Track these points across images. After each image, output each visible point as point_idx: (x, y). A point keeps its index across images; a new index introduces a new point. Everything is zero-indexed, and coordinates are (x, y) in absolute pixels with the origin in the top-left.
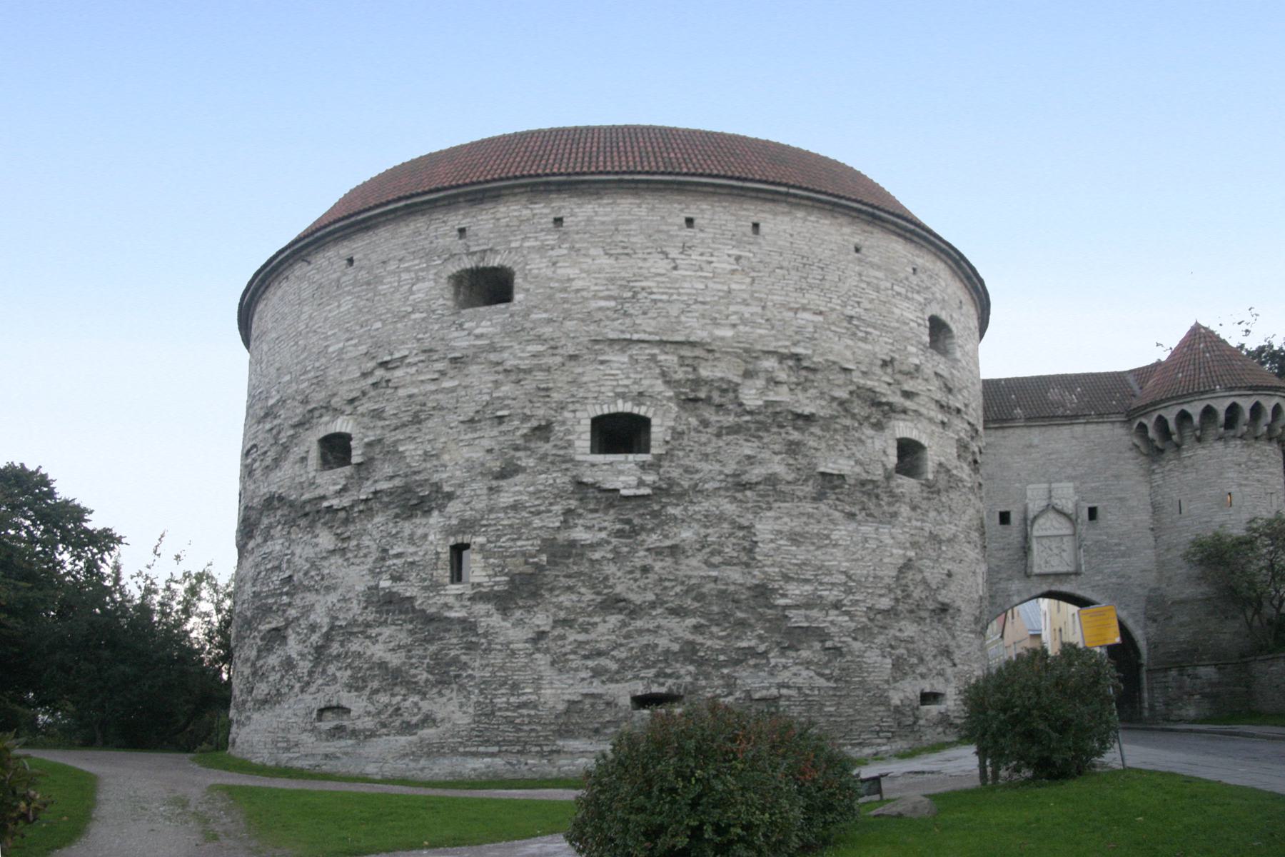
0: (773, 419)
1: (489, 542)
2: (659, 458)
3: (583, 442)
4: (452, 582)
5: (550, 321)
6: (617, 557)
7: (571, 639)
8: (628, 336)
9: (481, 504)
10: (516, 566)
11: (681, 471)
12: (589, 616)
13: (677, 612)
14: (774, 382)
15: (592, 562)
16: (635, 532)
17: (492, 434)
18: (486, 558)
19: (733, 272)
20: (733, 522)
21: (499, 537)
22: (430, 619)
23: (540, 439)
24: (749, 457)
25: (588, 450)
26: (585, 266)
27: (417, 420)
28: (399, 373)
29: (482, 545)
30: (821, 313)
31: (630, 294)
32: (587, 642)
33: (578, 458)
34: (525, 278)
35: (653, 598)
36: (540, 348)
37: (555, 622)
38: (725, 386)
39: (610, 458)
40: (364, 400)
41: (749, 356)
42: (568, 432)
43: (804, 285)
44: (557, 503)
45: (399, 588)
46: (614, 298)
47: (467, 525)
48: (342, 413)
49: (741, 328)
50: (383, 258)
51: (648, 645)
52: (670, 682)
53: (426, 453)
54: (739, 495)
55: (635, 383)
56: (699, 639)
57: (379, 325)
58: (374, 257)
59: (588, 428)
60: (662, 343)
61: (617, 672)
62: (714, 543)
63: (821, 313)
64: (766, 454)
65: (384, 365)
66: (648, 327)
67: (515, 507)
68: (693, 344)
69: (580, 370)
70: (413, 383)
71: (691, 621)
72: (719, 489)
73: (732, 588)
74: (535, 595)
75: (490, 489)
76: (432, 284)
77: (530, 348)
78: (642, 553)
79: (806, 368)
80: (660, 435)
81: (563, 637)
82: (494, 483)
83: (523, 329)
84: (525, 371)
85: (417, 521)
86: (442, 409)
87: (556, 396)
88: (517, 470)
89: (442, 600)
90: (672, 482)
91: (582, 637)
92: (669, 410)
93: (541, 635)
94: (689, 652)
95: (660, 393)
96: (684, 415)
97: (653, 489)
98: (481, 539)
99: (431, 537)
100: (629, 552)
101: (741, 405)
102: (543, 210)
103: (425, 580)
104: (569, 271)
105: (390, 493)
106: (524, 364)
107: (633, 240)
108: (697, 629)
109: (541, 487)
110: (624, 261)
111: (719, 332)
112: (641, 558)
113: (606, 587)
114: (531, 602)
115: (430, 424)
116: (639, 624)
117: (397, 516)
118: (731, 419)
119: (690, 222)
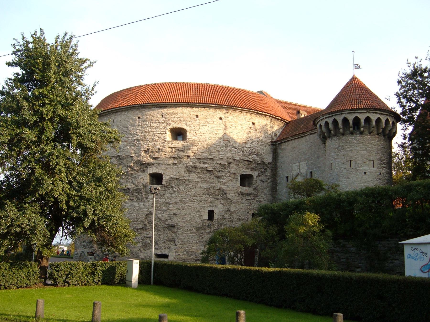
30: (126, 141)
63: (126, 141)
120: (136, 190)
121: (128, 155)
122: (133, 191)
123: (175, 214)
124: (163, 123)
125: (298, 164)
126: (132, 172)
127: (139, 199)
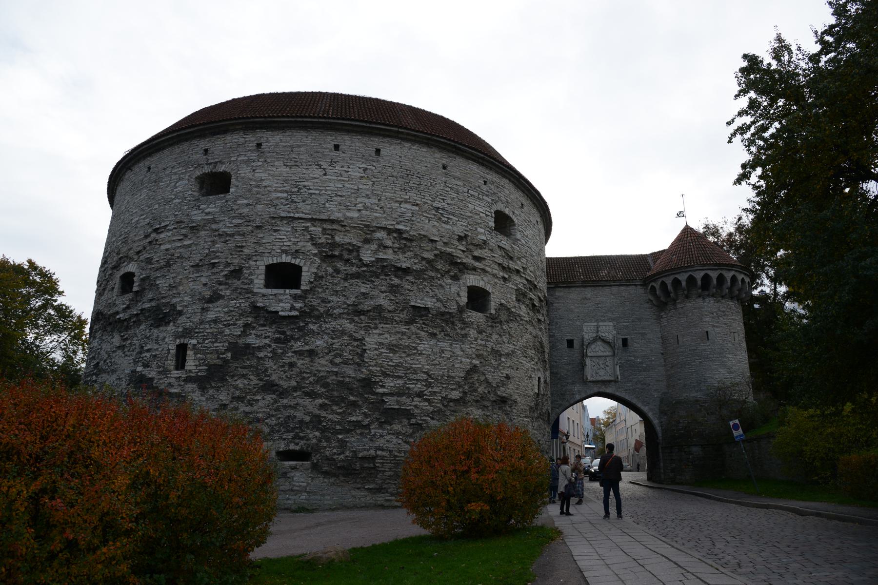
0: (383, 269)
1: (198, 343)
2: (306, 292)
3: (259, 281)
4: (177, 369)
5: (248, 205)
6: (275, 356)
7: (242, 410)
8: (292, 215)
9: (196, 319)
10: (212, 359)
11: (319, 301)
12: (254, 395)
13: (311, 395)
14: (382, 246)
15: (259, 358)
16: (286, 340)
17: (207, 274)
18: (195, 354)
19: (362, 177)
20: (351, 336)
21: (205, 340)
22: (160, 393)
23: (235, 278)
24: (364, 294)
25: (262, 286)
26: (271, 172)
27: (168, 265)
28: (162, 236)
29: (194, 345)
30: (417, 205)
31: (296, 190)
32: (251, 413)
33: (255, 290)
34: (237, 179)
35: (295, 384)
36: (240, 221)
37: (233, 398)
38: (351, 248)
39: (275, 291)
41: (368, 231)
42: (251, 274)
43: (407, 187)
44: (240, 319)
45: (146, 372)
46: (286, 192)
47: (188, 333)
49: (364, 212)
50: (164, 166)
51: (289, 417)
52: (302, 443)
53: (170, 285)
54: (356, 318)
55: (294, 244)
56: (324, 414)
57: (157, 206)
58: (160, 166)
59: (263, 272)
60: (312, 220)
61: (269, 434)
62: (337, 349)
63: (417, 205)
64: (375, 293)
65: (156, 231)
66: (305, 209)
67: (215, 321)
68: (332, 221)
69: (262, 235)
70: (169, 242)
71: (319, 401)
72: (343, 313)
73: (347, 380)
74: (223, 380)
75: (203, 309)
76: (186, 182)
77: (234, 221)
78: (290, 354)
79: (406, 239)
80: (307, 278)
81: (236, 409)
82: (206, 305)
83: (232, 209)
84: (230, 235)
85: (161, 328)
86: (182, 258)
87: (246, 251)
88: (220, 297)
89: (167, 381)
90: (313, 309)
91: (248, 409)
92: (314, 262)
93: (224, 406)
94: (316, 422)
95: (309, 251)
96: (324, 265)
97: (300, 312)
98: (194, 341)
99: (167, 339)
100: (282, 353)
101: (361, 260)
102: (251, 139)
103: (160, 367)
104: (261, 175)
105: (149, 310)
106: (229, 231)
107: (301, 157)
108: (322, 406)
109: (232, 309)
110: (294, 169)
111: (348, 214)
112: (289, 357)
113: (266, 376)
114: (220, 385)
115: (175, 267)
116: (285, 401)
117: (152, 325)
118: (354, 269)
119: (337, 147)
120: (443, 314)
121: (425, 236)
122: (437, 315)
123: (508, 377)
124: (487, 196)
125: (595, 324)
126: (433, 274)
127: (448, 335)
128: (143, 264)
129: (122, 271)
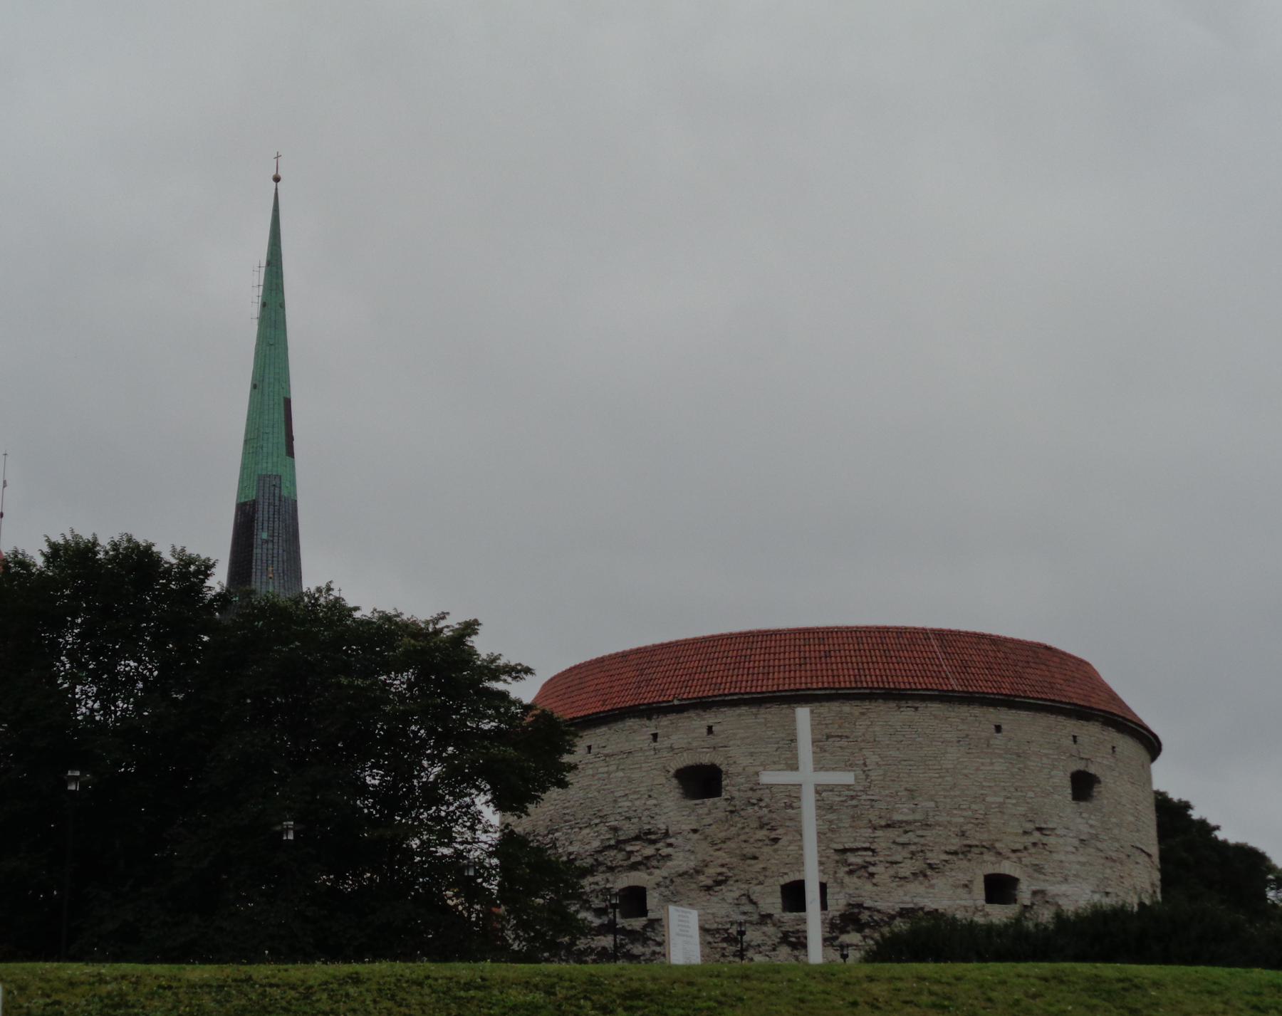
40: (1025, 854)
48: (1008, 858)
57: (1031, 794)
65: (1040, 829)
128: (1030, 870)
129: (990, 870)
